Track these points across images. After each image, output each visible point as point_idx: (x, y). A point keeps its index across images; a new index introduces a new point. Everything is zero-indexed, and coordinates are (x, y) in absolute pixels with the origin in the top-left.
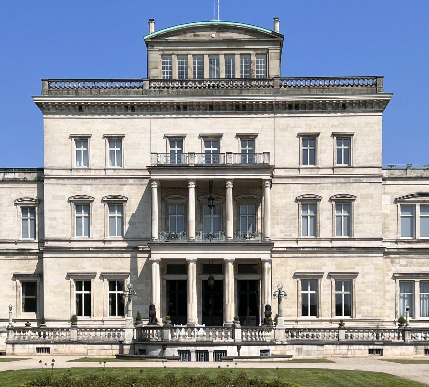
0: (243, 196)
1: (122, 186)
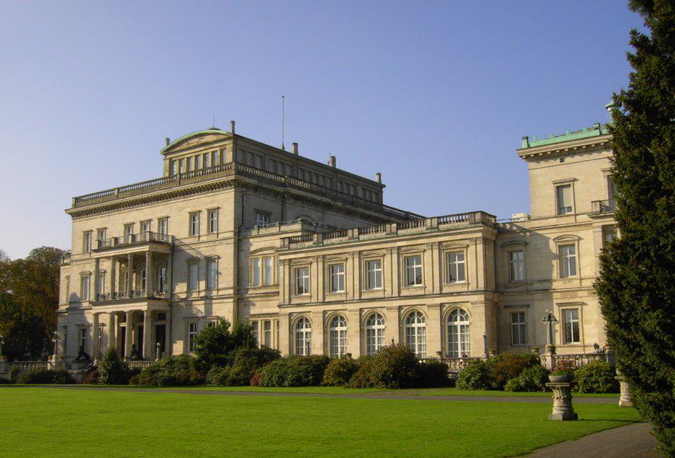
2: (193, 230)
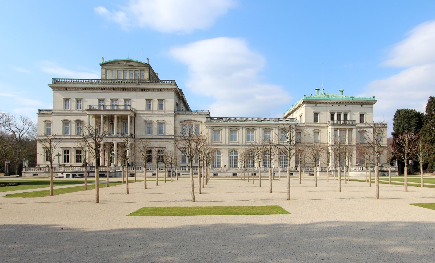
0: (125, 120)
1: (81, 116)
2: (148, 107)
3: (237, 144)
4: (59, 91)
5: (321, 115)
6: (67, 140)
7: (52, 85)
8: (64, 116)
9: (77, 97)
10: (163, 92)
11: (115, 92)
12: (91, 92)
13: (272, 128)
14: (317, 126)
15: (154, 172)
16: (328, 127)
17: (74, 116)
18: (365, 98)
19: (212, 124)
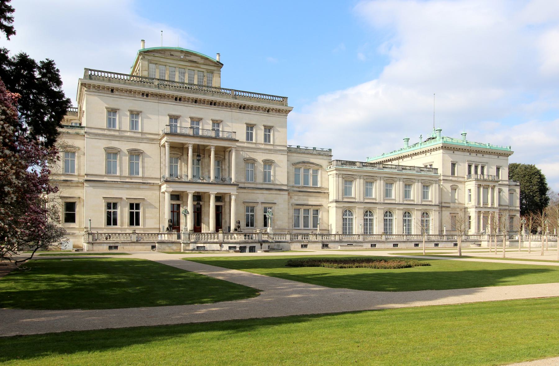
3: (374, 201)
4: (98, 92)
5: (459, 166)
6: (115, 186)
7: (84, 80)
8: (108, 141)
9: (132, 109)
10: (271, 115)
11: (197, 106)
12: (157, 101)
13: (414, 180)
14: (455, 181)
15: (304, 242)
16: (466, 183)
17: (126, 142)
18: (502, 148)
19: (343, 170)
